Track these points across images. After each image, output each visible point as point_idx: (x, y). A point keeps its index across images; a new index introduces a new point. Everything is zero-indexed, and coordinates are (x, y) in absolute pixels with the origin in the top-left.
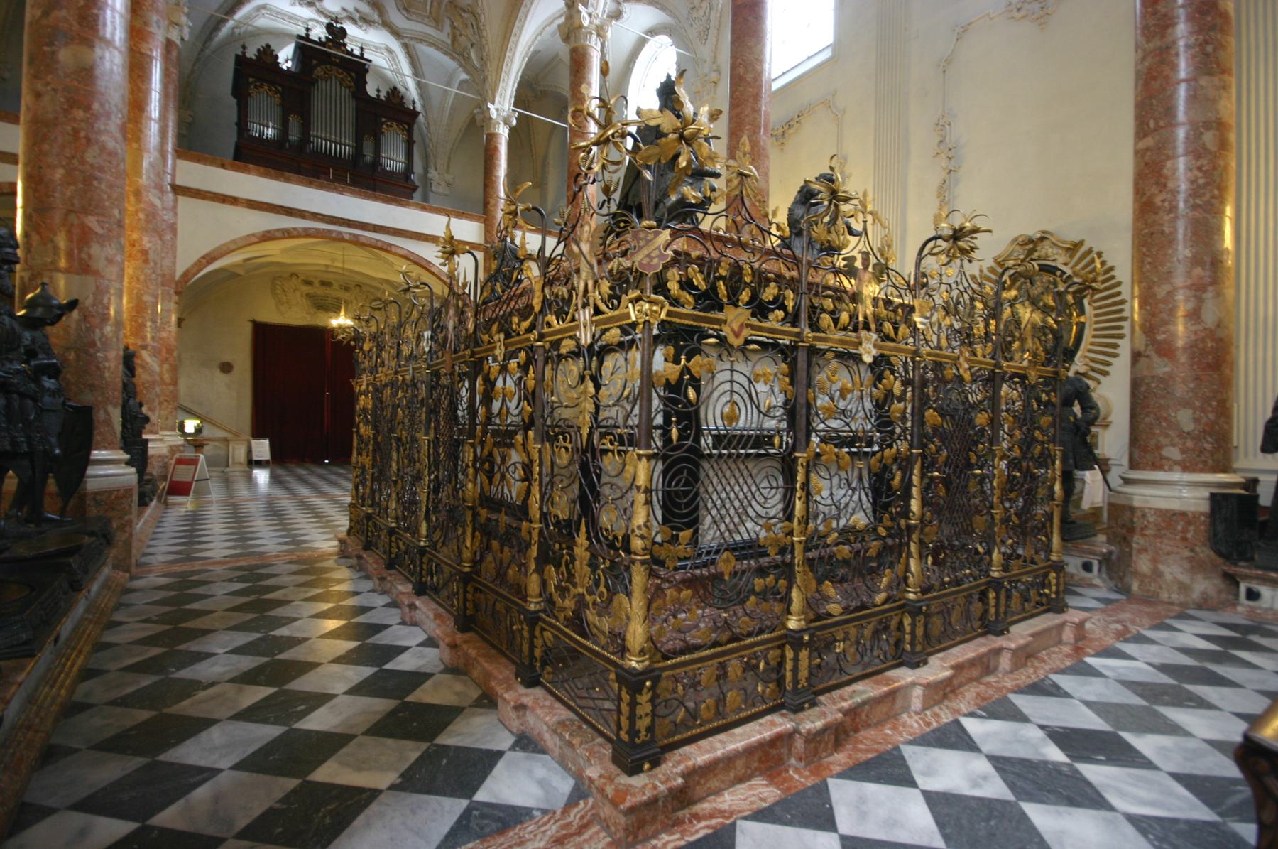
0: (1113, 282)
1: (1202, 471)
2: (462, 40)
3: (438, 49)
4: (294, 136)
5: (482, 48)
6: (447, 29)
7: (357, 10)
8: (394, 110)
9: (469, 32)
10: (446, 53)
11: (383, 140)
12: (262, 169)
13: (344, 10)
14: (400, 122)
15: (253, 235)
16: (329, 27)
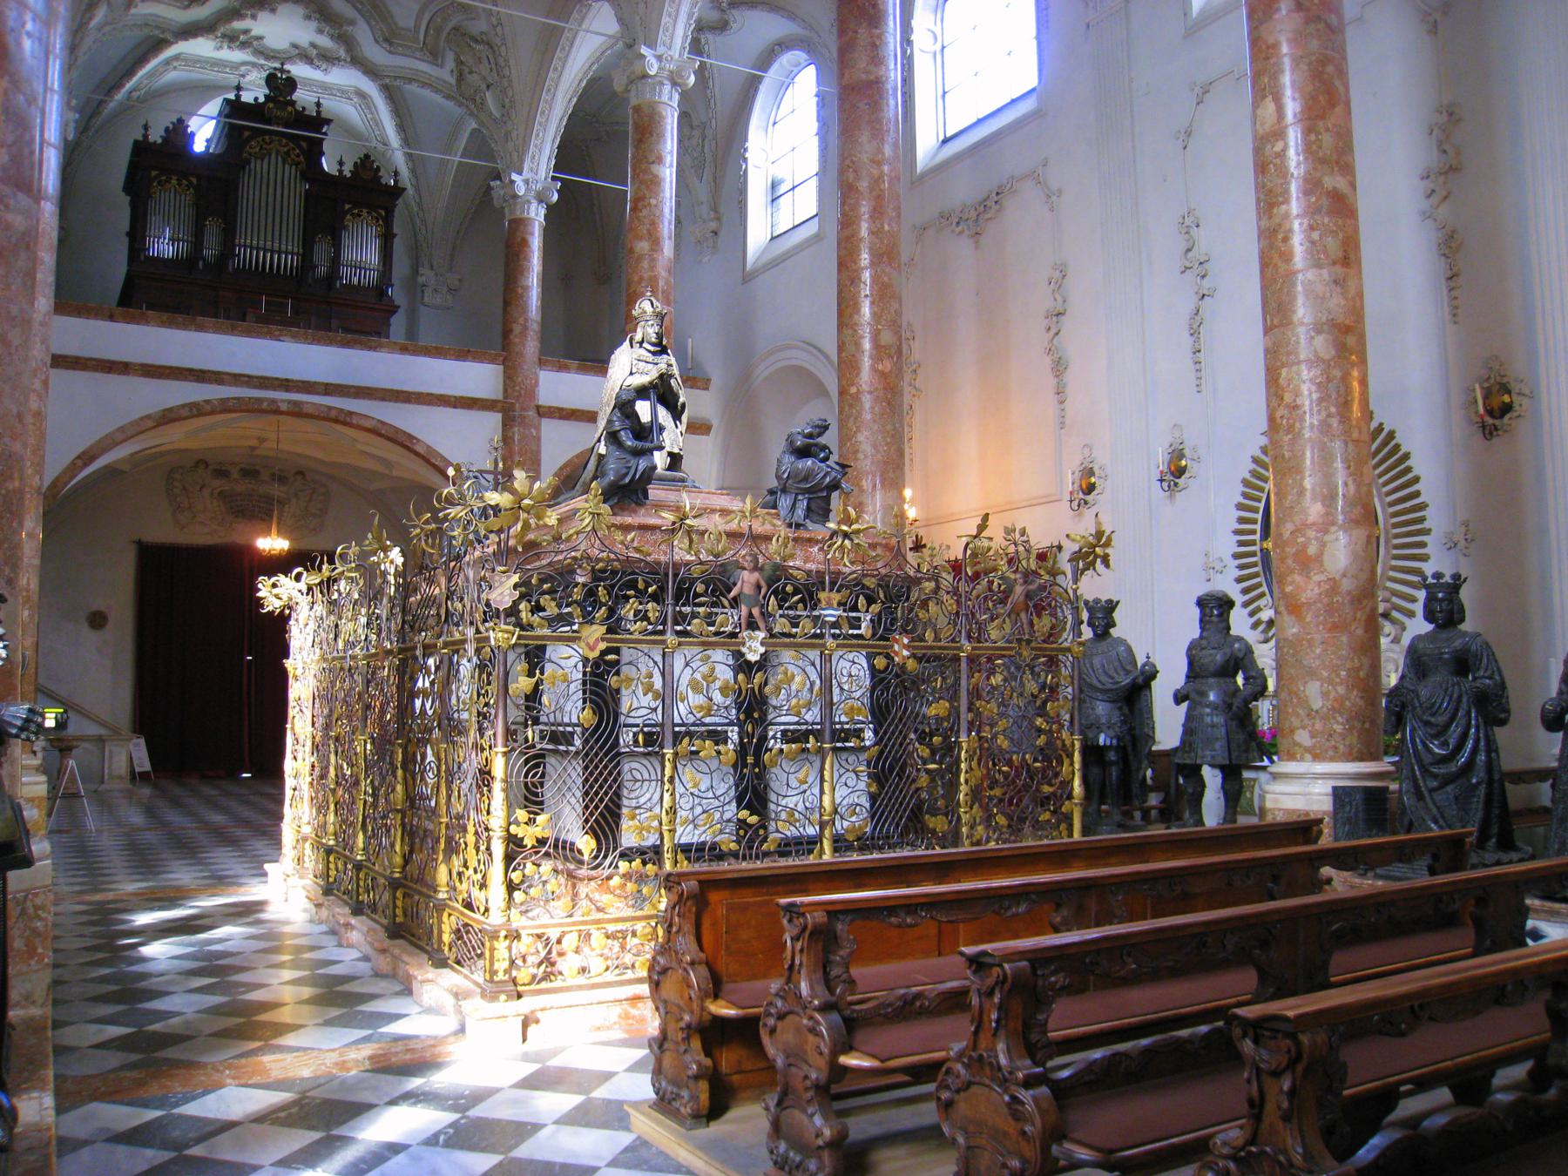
0: (1410, 476)
1: (1332, 759)
2: (474, 79)
3: (437, 91)
4: (210, 252)
5: (504, 91)
6: (450, 63)
7: (313, 45)
8: (368, 191)
9: (484, 68)
10: (448, 97)
11: (346, 240)
12: (165, 316)
13: (295, 46)
14: (372, 208)
15: (149, 417)
16: (271, 80)
